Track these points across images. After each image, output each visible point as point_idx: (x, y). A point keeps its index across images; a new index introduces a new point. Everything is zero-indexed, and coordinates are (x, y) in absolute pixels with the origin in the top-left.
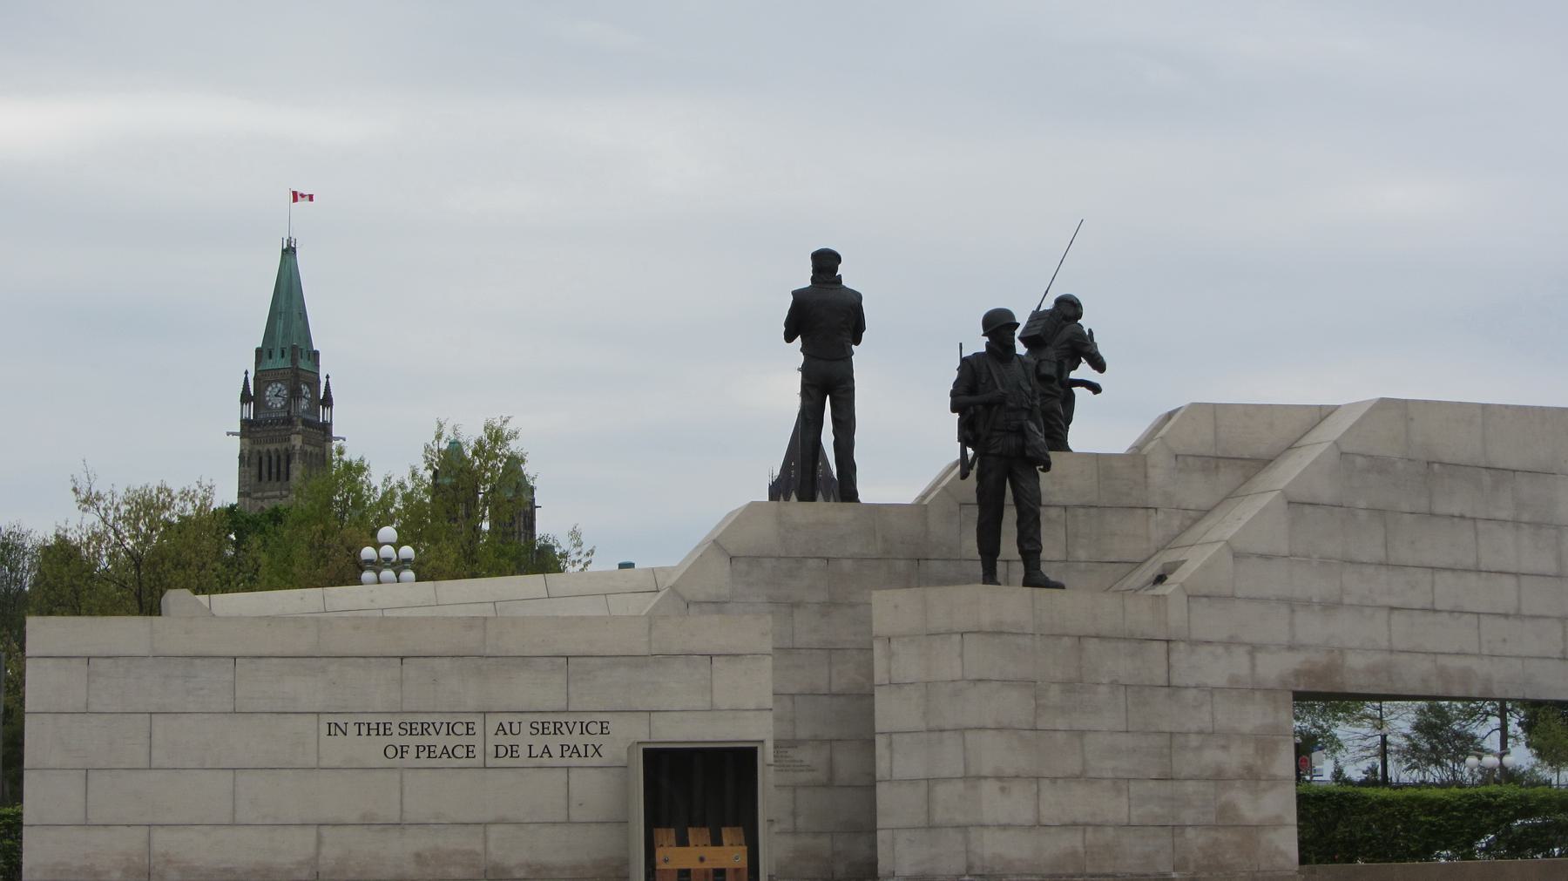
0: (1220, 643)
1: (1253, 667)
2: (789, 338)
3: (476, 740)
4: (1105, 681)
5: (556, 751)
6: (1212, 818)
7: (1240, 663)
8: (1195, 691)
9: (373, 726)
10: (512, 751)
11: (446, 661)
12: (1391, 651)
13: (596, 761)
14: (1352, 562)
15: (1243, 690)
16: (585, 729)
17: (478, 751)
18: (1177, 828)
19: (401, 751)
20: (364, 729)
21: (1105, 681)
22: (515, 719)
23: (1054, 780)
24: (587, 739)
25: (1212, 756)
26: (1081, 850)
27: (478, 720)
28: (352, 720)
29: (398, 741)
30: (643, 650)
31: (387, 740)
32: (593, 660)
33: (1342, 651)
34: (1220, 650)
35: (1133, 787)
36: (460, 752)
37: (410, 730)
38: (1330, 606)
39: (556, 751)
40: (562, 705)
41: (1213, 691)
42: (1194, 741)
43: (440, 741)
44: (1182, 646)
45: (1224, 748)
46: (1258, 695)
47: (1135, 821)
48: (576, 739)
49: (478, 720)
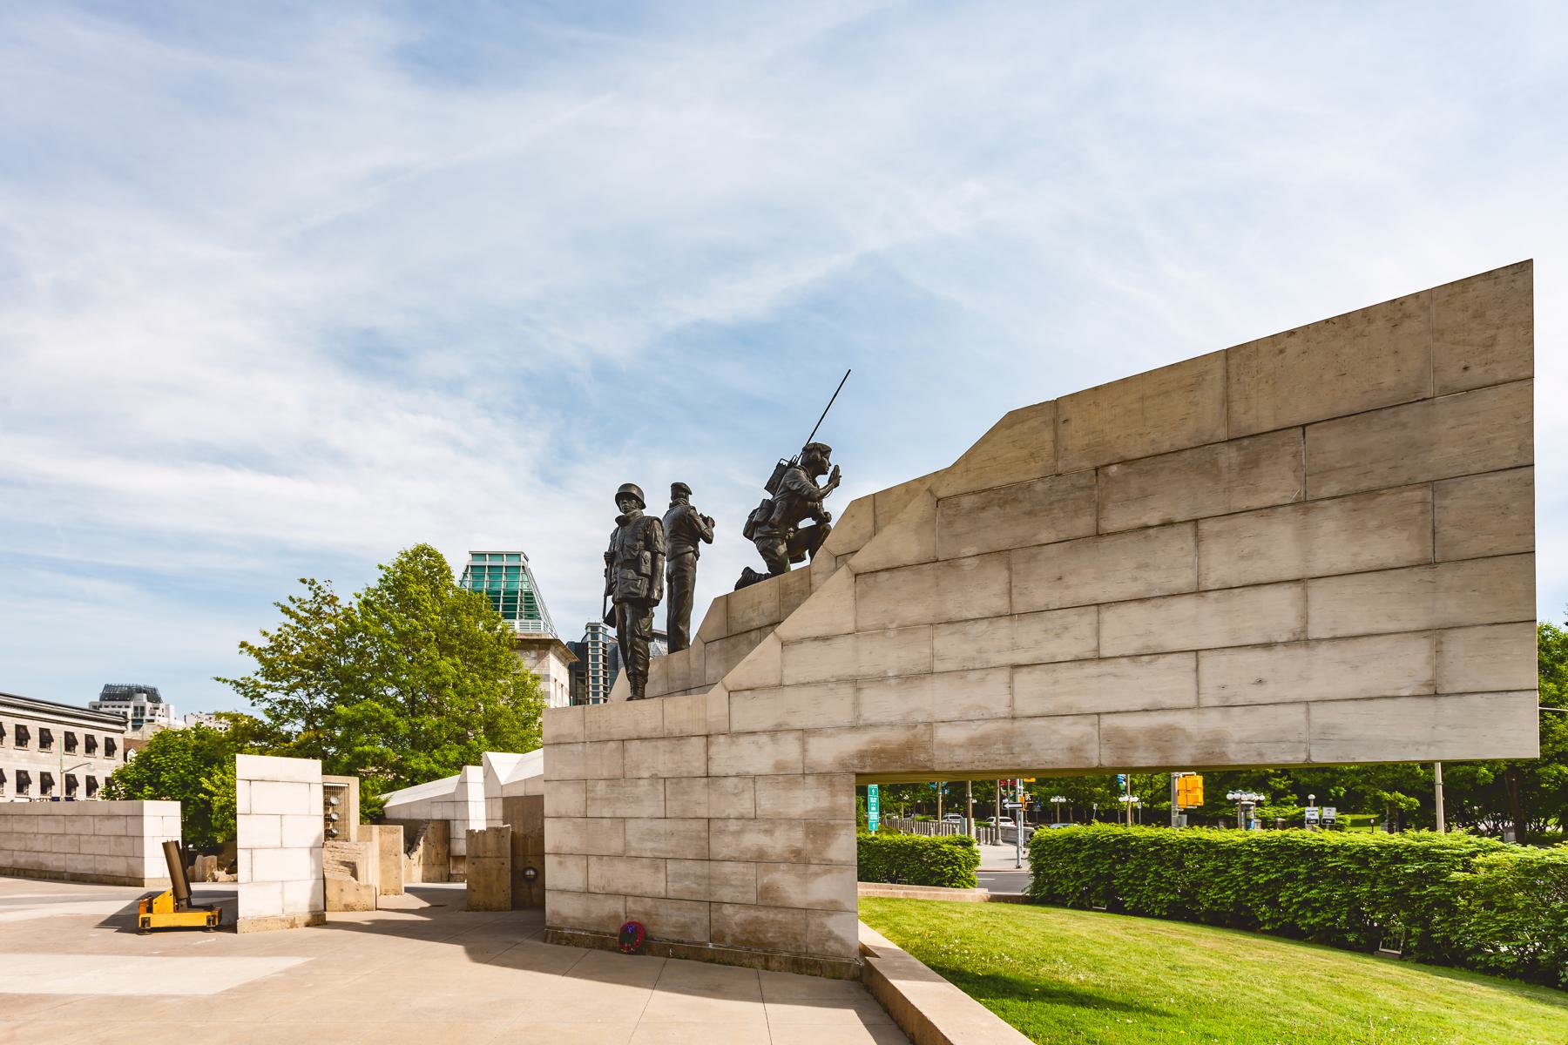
0: (764, 732)
1: (804, 751)
4: (645, 774)
6: (752, 897)
7: (789, 749)
8: (735, 780)
12: (1014, 718)
14: (949, 622)
15: (785, 777)
18: (713, 904)
21: (645, 774)
23: (601, 857)
25: (753, 840)
26: (622, 914)
33: (929, 725)
34: (764, 739)
35: (671, 866)
38: (908, 678)
41: (755, 778)
42: (733, 826)
44: (722, 739)
45: (769, 832)
46: (810, 780)
47: (671, 894)
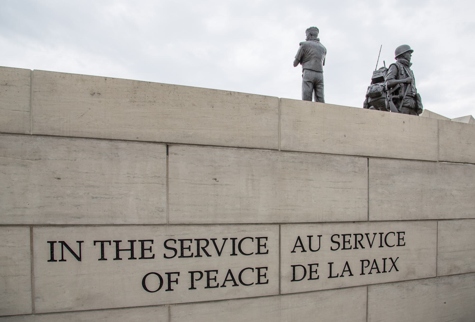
2: (295, 65)
3: (269, 261)
5: (356, 267)
9: (125, 245)
10: (311, 272)
11: (229, 152)
13: (392, 276)
16: (384, 242)
17: (272, 275)
19: (168, 281)
20: (110, 251)
22: (315, 231)
24: (386, 252)
27: (271, 233)
28: (89, 236)
29: (162, 265)
30: (431, 155)
31: (148, 266)
32: (392, 162)
36: (250, 277)
37: (179, 249)
39: (356, 267)
40: (363, 217)
43: (223, 263)
48: (375, 253)
49: (271, 233)
